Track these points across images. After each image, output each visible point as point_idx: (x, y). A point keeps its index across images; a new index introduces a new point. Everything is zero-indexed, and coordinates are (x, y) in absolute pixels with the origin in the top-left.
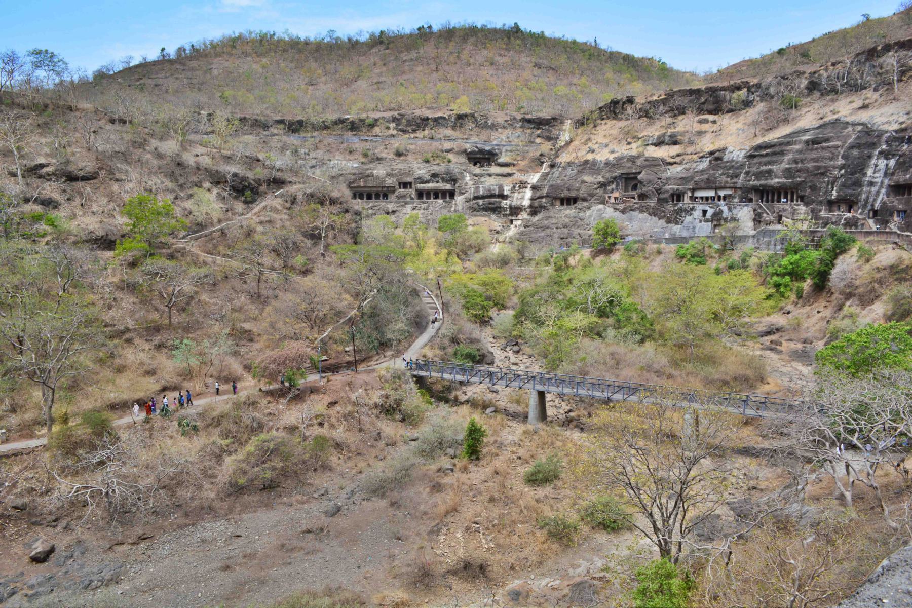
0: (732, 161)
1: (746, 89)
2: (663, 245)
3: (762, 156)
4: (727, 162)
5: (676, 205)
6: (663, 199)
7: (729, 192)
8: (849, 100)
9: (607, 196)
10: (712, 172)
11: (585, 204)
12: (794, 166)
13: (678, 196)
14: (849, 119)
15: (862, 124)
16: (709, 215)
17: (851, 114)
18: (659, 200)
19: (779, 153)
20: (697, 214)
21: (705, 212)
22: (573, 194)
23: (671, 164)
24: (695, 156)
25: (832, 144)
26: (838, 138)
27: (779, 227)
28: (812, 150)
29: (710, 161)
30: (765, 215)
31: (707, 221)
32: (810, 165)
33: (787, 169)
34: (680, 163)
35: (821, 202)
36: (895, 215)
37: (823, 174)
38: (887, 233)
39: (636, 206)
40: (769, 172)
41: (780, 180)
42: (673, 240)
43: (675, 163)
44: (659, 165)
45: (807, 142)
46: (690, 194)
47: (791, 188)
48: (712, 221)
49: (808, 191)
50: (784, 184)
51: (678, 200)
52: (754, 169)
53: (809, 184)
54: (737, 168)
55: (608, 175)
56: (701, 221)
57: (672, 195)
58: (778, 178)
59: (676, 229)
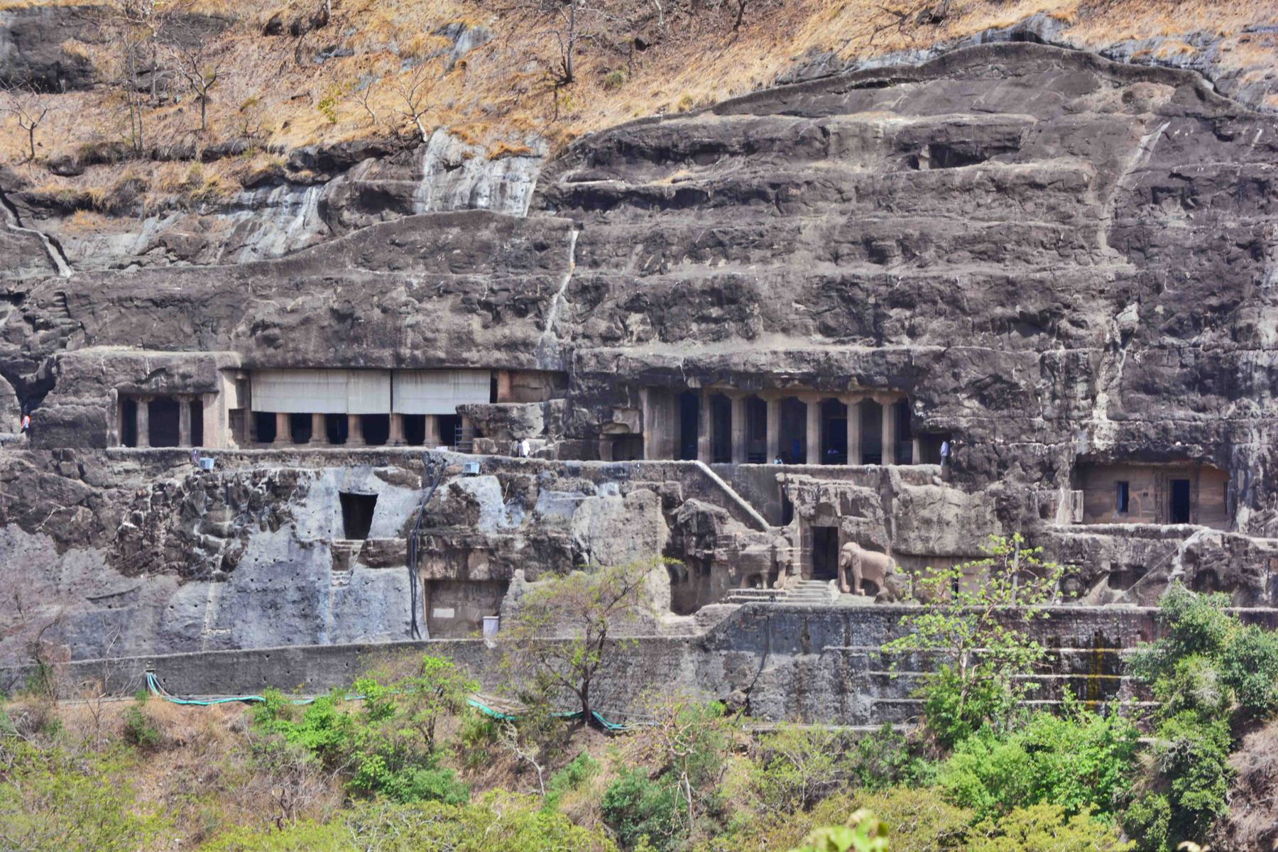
0: (472, 217)
2: (159, 705)
4: (440, 222)
5: (167, 462)
7: (475, 395)
10: (360, 275)
12: (867, 269)
13: (165, 414)
14: (1078, 37)
15: (1166, 73)
18: (40, 431)
19: (760, 195)
20: (318, 516)
21: (358, 510)
24: (209, 172)
25: (1025, 168)
26: (1065, 139)
27: (832, 595)
28: (944, 191)
29: (325, 209)
30: (734, 528)
31: (379, 558)
32: (966, 273)
33: (828, 285)
34: (120, 207)
35: (1048, 470)
37: (1030, 324)
41: (798, 344)
42: (220, 670)
43: (86, 204)
45: (904, 146)
48: (413, 559)
51: (164, 431)
52: (624, 273)
53: (971, 373)
54: (518, 262)
56: (340, 560)
57: (127, 403)
58: (785, 331)
59: (197, 602)
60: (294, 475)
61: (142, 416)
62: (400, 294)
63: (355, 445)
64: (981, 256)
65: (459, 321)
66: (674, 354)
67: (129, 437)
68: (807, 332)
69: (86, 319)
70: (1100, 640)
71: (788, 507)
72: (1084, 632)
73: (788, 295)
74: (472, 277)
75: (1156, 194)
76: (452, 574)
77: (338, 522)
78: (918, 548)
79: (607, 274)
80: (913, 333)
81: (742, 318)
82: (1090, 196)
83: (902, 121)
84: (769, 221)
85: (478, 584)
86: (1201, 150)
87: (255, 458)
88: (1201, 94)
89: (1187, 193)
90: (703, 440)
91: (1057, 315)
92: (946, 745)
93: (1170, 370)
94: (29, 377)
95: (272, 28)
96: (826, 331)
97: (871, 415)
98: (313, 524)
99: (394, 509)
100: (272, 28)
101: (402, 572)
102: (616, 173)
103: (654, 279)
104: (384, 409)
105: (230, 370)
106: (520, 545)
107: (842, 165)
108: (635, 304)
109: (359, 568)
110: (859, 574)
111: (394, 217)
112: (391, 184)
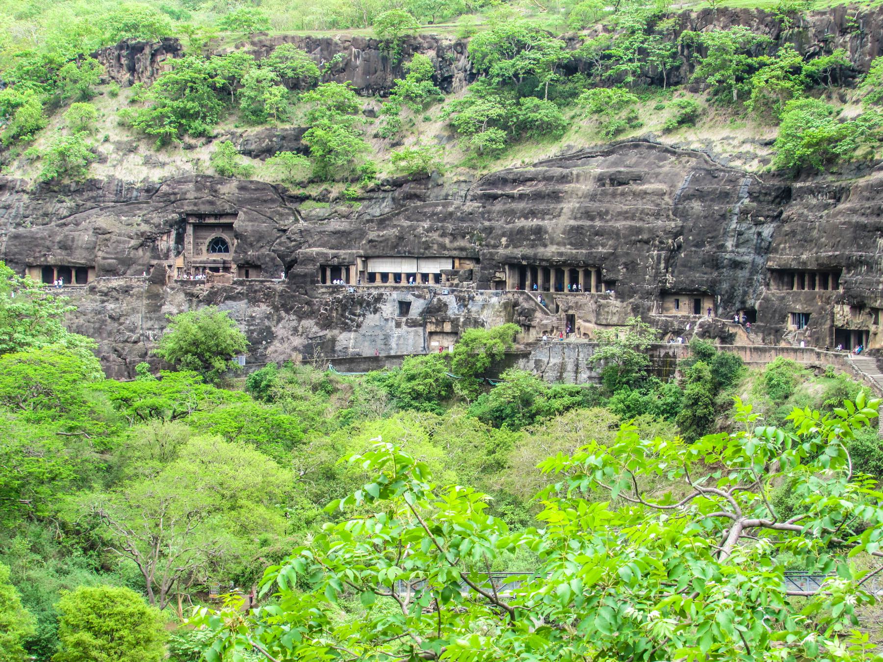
1: (432, 53)
3: (512, 197)
6: (305, 275)
7: (447, 266)
8: (653, 104)
9: (165, 263)
11: (116, 282)
12: (589, 223)
15: (693, 154)
16: (415, 311)
17: (668, 131)
20: (389, 309)
21: (405, 307)
22: (79, 258)
23: (302, 199)
27: (573, 338)
28: (614, 195)
31: (413, 324)
32: (620, 224)
33: (573, 228)
36: (790, 319)
38: (783, 350)
39: (239, 288)
40: (539, 231)
41: (562, 249)
43: (307, 198)
44: (273, 201)
45: (600, 180)
46: (360, 267)
47: (586, 265)
48: (424, 325)
49: (622, 270)
50: (575, 257)
52: (500, 224)
53: (623, 260)
54: (462, 220)
55: (157, 218)
56: (398, 325)
57: (323, 268)
60: (382, 294)
61: (328, 273)
62: (420, 230)
63: (404, 283)
64: (626, 218)
65: (441, 240)
66: (519, 252)
67: (324, 281)
68: (565, 245)
69: (309, 239)
70: (667, 355)
71: (558, 306)
72: (663, 352)
73: (558, 232)
74: (446, 225)
75: (688, 197)
76: (438, 330)
77: (397, 312)
78: (604, 322)
79: (494, 223)
80: (603, 246)
81: (540, 239)
82: (666, 198)
83: (599, 171)
84: (552, 206)
85: (447, 333)
86: (706, 182)
87: (368, 288)
88: (706, 162)
89: (700, 195)
90: (528, 283)
91: (654, 239)
92: (612, 392)
93: (696, 260)
94: (289, 259)
95: (376, 136)
96: (571, 244)
97: (587, 275)
98: (389, 312)
99: (417, 307)
100: (376, 136)
101: (420, 329)
102: (497, 188)
103: (511, 226)
104: (414, 270)
105: (361, 257)
106: (462, 320)
107: (578, 186)
108: (503, 235)
109: (404, 327)
110: (582, 331)
111: (419, 203)
112: (418, 192)
